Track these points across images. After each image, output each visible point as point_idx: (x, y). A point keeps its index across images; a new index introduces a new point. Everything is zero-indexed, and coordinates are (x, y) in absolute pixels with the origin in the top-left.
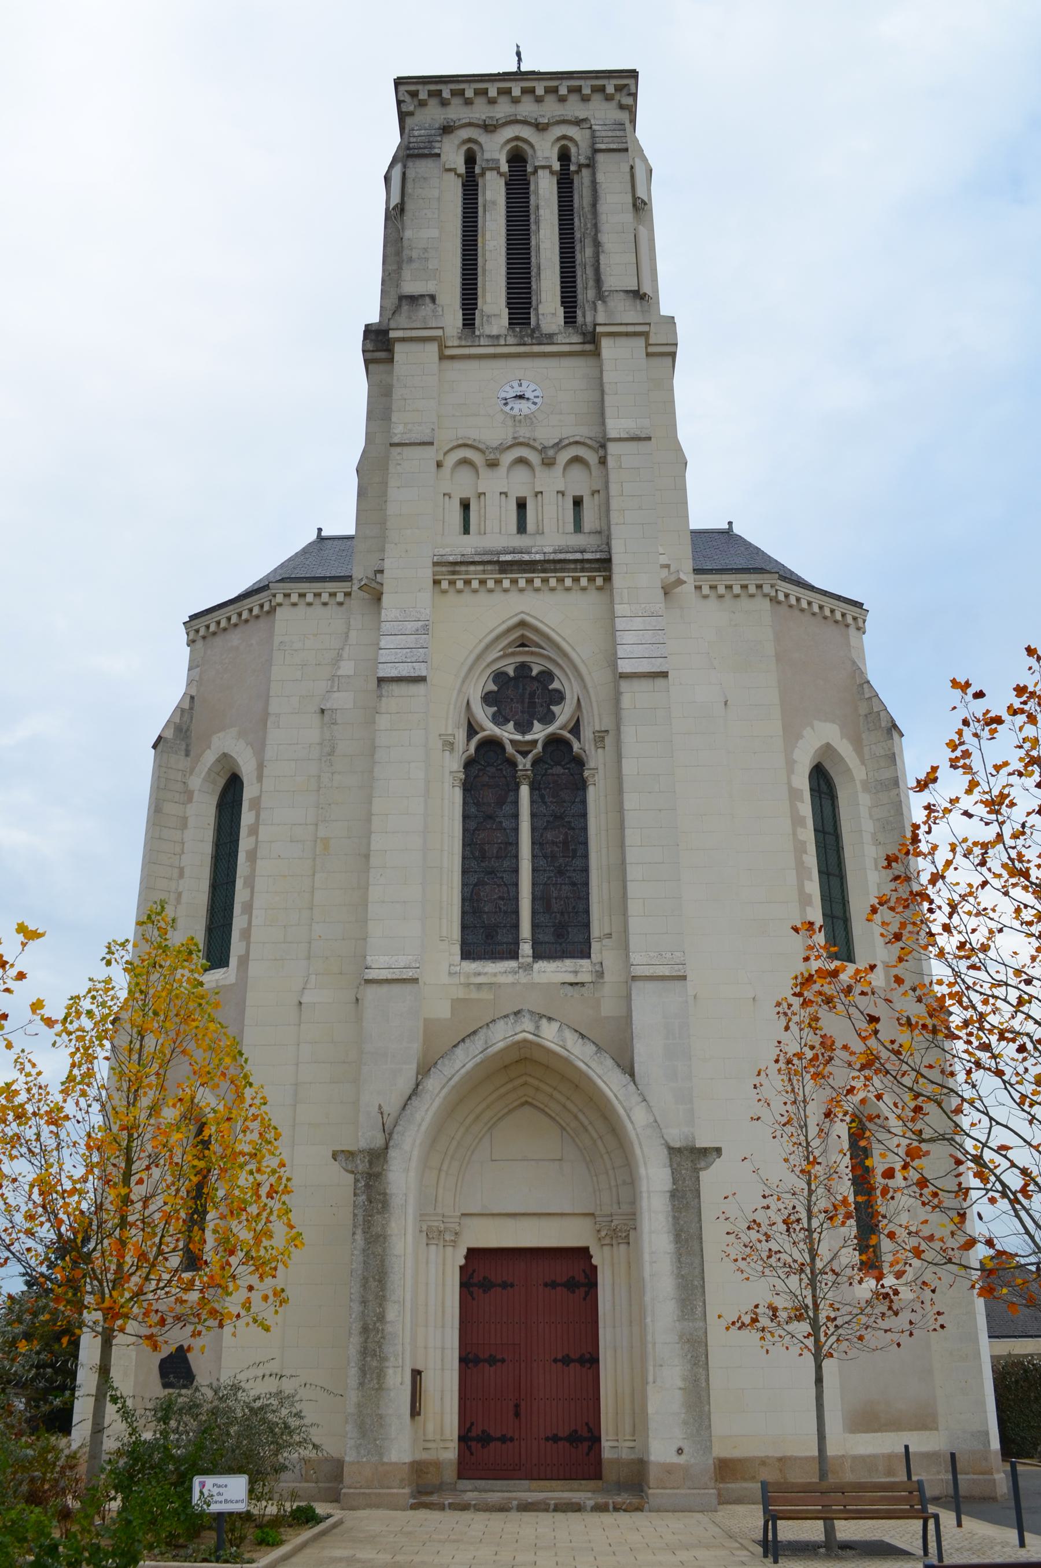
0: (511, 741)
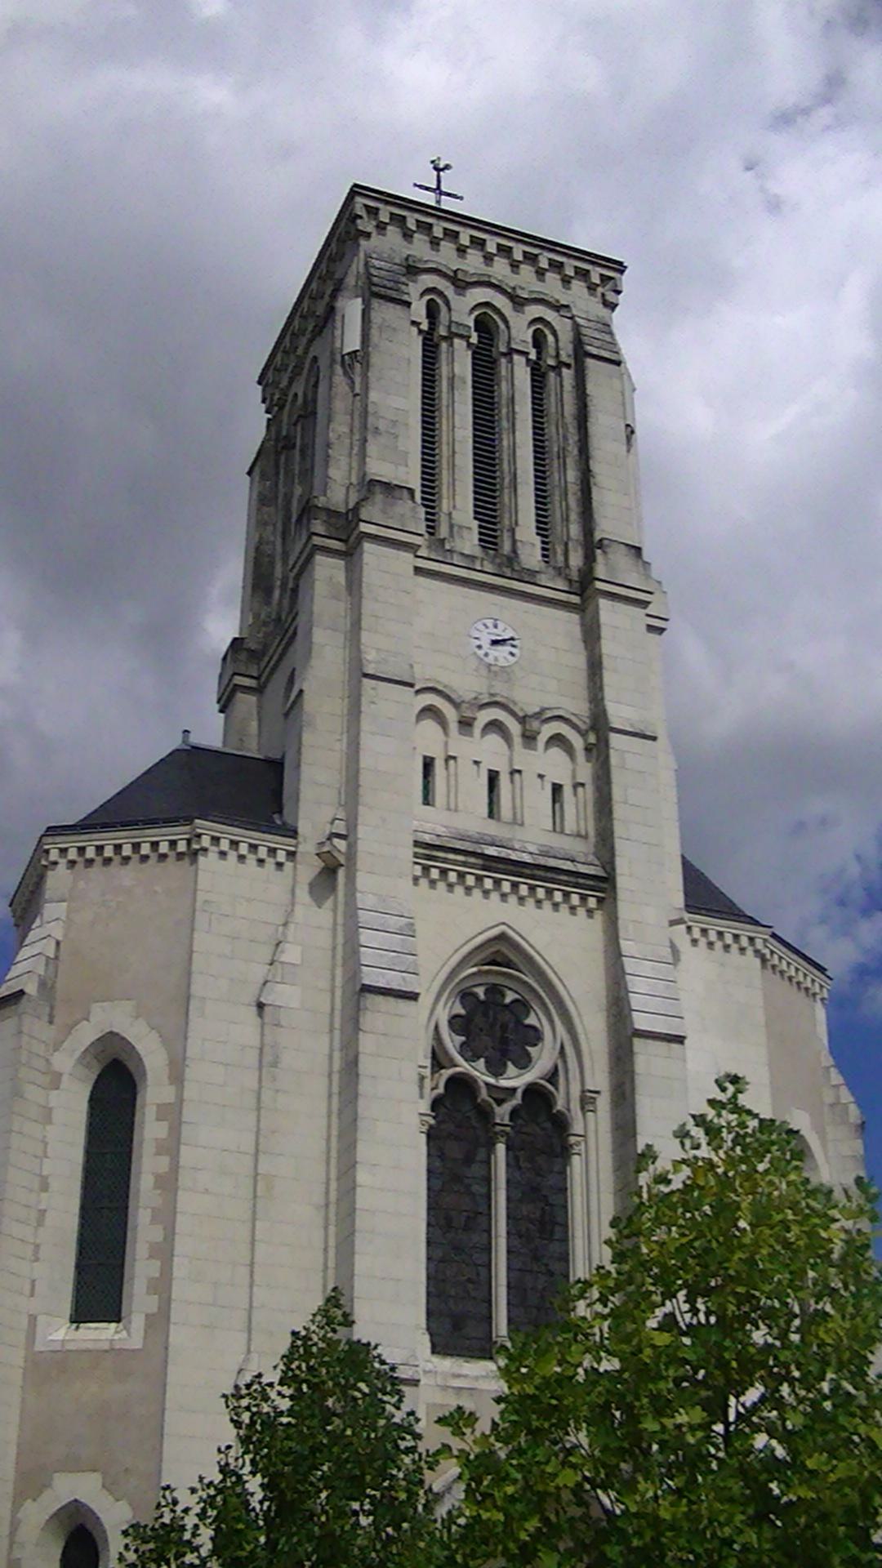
0: (487, 1084)
